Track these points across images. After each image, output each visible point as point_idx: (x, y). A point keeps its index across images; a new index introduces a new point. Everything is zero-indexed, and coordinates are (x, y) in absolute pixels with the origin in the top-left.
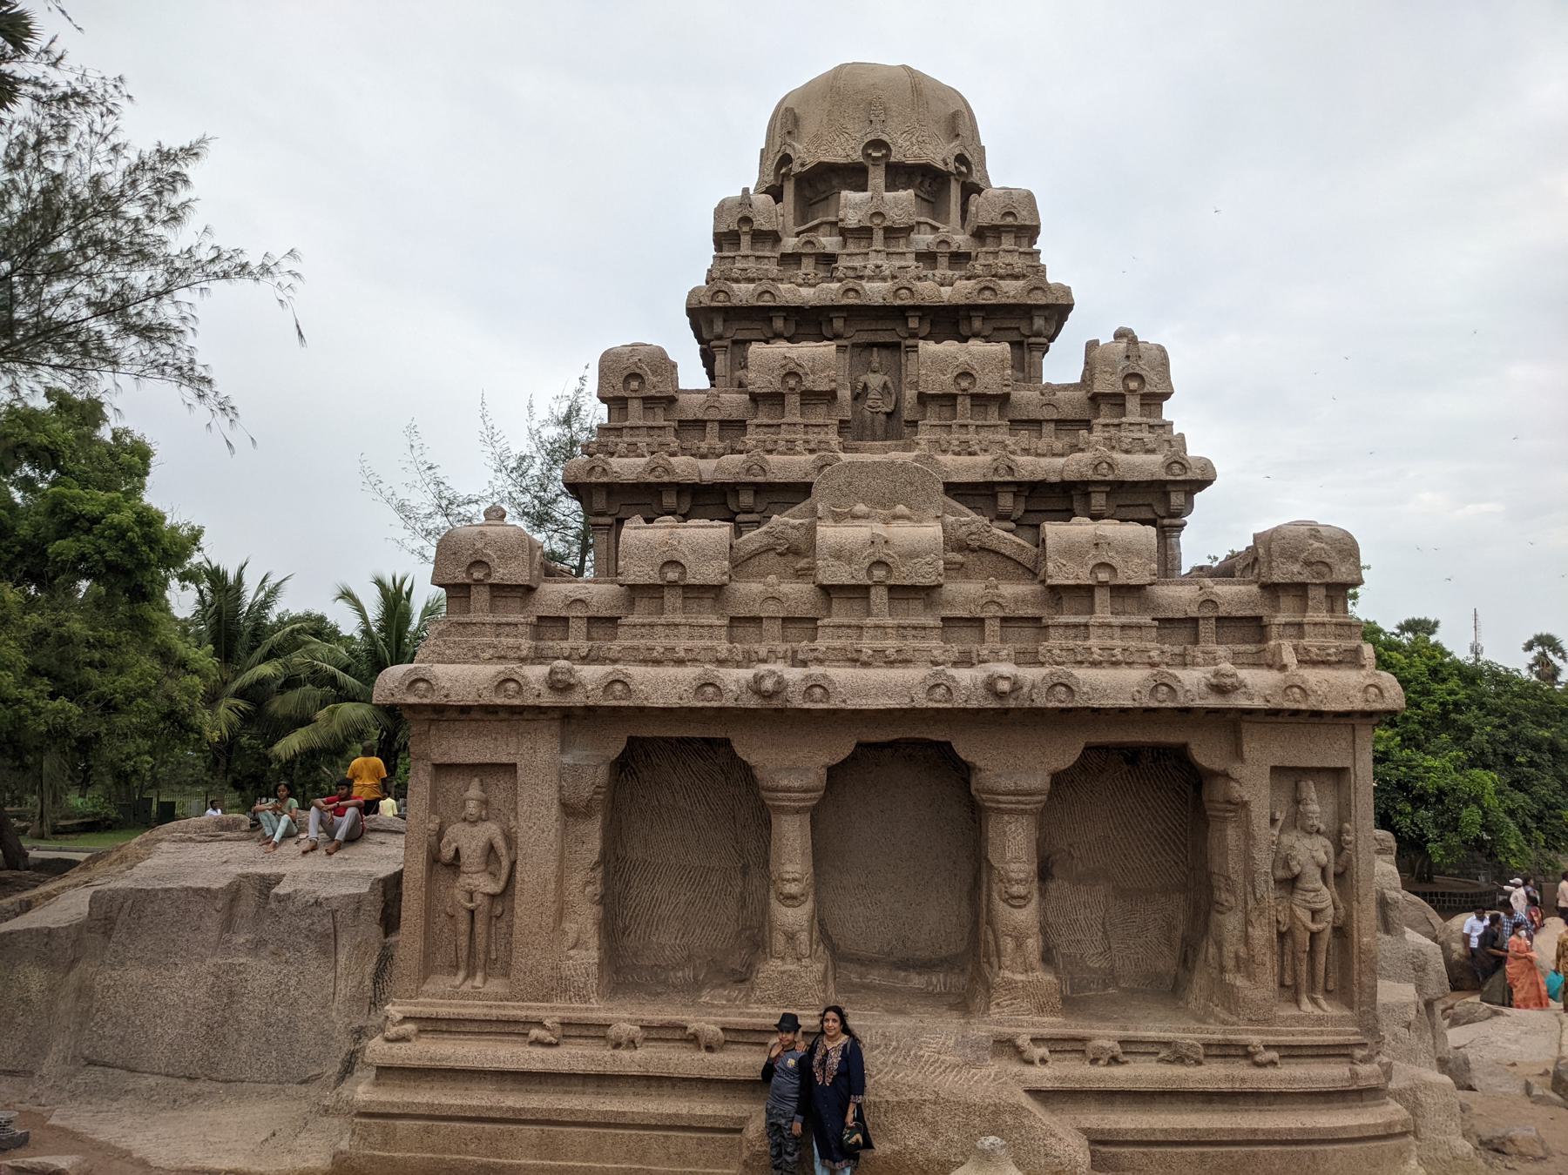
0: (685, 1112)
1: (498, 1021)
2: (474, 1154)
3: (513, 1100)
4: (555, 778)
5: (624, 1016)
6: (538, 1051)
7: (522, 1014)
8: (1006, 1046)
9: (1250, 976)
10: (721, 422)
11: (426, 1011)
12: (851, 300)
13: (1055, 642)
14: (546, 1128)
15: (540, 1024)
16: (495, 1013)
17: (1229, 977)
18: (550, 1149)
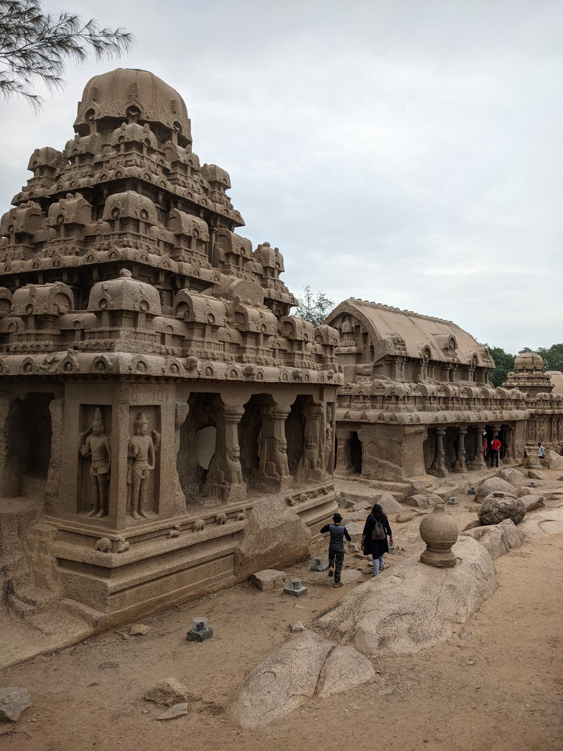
0: (219, 551)
1: (160, 530)
2: (154, 596)
3: (168, 566)
4: (174, 412)
5: (198, 517)
6: (175, 540)
7: (167, 525)
8: (289, 503)
9: (321, 468)
10: (164, 242)
11: (133, 533)
12: (189, 198)
13: (297, 360)
14: (179, 574)
15: (174, 528)
16: (157, 527)
17: (316, 469)
18: (180, 583)
